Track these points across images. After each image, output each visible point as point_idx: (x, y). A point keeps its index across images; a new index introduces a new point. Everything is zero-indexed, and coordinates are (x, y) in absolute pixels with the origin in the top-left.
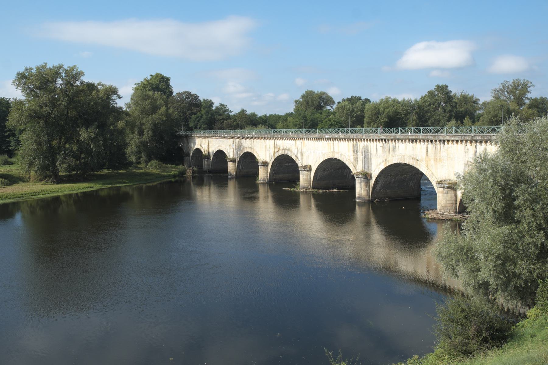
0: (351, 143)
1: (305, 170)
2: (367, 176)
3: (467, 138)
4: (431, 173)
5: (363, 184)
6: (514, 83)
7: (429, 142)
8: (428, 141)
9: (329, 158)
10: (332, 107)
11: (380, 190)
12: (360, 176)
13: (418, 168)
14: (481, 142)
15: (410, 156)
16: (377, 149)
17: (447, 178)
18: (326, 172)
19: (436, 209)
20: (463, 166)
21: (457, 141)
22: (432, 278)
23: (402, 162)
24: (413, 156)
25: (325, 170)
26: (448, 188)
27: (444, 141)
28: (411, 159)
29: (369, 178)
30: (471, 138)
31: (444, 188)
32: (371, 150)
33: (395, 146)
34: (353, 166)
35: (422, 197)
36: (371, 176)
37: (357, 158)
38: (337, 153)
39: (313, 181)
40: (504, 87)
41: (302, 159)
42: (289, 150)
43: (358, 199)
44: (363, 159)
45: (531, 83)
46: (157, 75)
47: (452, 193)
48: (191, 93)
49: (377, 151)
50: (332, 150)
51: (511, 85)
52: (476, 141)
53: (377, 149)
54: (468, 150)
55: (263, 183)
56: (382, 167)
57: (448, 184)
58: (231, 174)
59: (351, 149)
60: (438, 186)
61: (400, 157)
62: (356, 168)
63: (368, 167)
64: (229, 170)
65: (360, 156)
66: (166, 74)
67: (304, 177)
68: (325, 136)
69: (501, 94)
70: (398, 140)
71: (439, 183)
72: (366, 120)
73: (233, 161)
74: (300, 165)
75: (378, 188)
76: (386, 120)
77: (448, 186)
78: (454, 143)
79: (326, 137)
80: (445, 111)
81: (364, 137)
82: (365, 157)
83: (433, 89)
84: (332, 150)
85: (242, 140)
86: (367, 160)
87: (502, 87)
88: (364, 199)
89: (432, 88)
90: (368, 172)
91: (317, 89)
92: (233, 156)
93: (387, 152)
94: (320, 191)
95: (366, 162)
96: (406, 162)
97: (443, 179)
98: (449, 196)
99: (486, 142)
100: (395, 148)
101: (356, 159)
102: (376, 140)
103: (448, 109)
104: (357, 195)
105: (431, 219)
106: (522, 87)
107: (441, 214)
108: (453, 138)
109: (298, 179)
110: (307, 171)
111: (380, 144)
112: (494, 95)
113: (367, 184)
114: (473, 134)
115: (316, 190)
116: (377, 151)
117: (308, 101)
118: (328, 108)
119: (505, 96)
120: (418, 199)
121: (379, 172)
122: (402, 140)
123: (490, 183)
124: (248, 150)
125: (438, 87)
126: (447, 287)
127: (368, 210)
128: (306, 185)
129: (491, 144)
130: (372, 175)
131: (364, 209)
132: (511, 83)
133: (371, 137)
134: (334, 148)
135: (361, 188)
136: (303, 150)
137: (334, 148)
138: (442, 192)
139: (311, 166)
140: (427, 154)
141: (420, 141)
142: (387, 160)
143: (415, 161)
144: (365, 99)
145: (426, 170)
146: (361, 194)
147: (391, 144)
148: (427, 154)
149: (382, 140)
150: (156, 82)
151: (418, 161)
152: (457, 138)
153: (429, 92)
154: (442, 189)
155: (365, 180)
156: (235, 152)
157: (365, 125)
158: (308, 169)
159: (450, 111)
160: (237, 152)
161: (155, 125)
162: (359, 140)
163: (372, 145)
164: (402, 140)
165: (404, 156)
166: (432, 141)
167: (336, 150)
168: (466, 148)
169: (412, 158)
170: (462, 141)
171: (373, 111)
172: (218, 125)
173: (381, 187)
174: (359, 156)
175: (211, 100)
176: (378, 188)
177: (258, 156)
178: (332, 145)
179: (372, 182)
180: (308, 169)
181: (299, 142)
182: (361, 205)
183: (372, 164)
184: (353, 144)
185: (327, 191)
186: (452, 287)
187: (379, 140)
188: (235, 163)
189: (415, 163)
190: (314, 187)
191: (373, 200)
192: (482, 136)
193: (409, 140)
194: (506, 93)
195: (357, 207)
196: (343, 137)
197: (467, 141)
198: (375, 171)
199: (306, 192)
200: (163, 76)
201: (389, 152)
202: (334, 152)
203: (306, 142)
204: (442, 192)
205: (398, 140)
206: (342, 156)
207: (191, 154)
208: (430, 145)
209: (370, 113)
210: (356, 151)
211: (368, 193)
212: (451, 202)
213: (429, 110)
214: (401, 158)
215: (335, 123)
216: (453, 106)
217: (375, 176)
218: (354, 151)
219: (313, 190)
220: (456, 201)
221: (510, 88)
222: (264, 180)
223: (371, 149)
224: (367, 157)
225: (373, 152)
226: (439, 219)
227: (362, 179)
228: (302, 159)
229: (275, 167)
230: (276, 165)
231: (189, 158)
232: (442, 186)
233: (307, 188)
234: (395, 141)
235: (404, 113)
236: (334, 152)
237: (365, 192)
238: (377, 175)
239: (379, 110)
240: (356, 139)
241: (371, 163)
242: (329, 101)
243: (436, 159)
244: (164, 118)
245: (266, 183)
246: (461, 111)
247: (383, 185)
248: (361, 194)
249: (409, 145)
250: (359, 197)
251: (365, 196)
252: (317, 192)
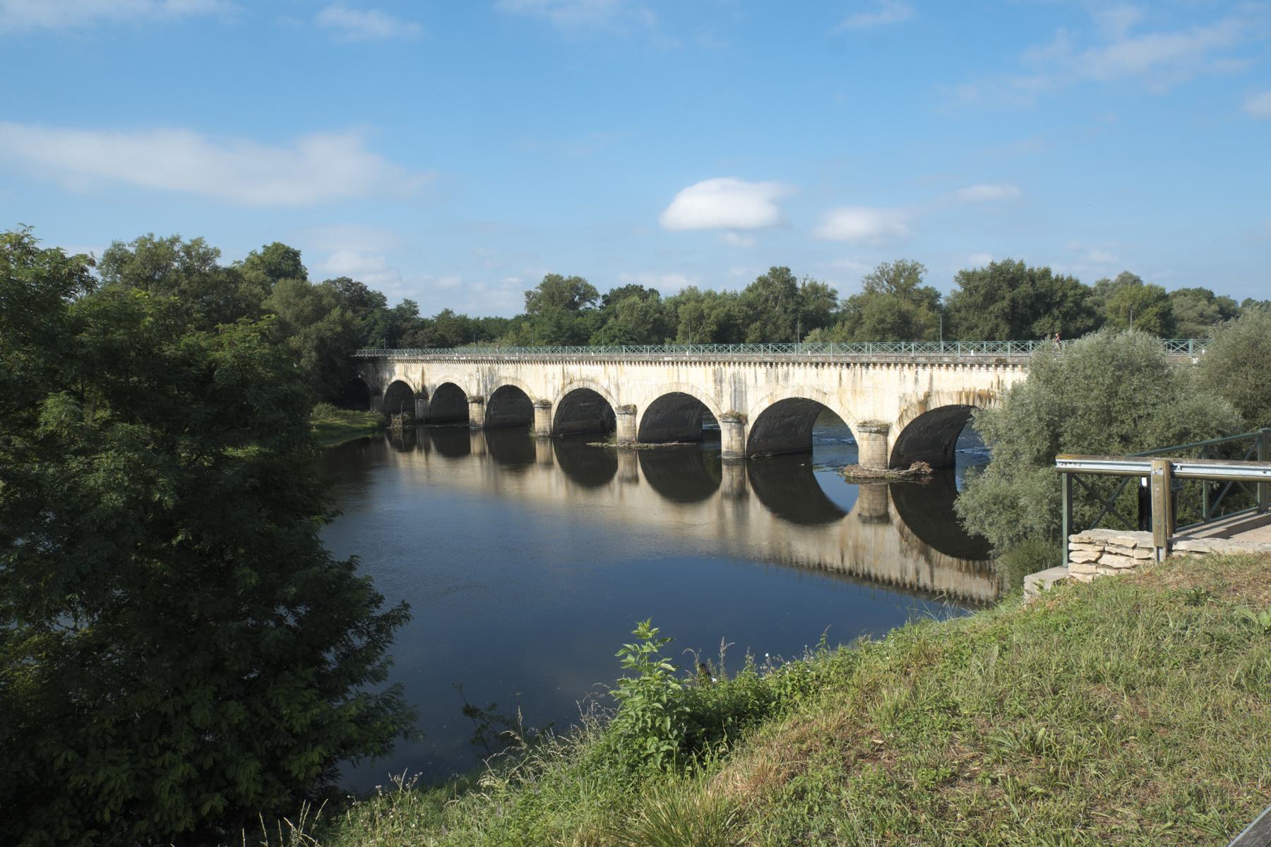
0: (710, 369)
1: (627, 413)
2: (740, 420)
3: (905, 360)
4: (846, 411)
5: (734, 431)
6: (897, 266)
7: (844, 366)
8: (842, 364)
9: (670, 392)
10: (594, 304)
11: (758, 440)
12: (730, 420)
13: (825, 404)
14: (925, 365)
17: (872, 419)
19: (858, 463)
20: (898, 400)
21: (889, 365)
22: (848, 564)
23: (800, 396)
25: (658, 412)
26: (877, 432)
27: (868, 365)
29: (744, 422)
30: (910, 360)
31: (871, 432)
32: (745, 380)
33: (788, 373)
34: (713, 404)
35: (814, 449)
36: (746, 418)
37: (721, 391)
38: (684, 384)
39: (640, 430)
40: (882, 272)
41: (618, 395)
42: (592, 380)
43: (727, 455)
45: (922, 266)
46: (277, 246)
49: (756, 381)
51: (892, 270)
52: (917, 365)
55: (544, 436)
56: (766, 404)
57: (877, 426)
58: (475, 424)
59: (711, 378)
60: (861, 430)
61: (796, 388)
62: (719, 407)
63: (741, 405)
64: (471, 417)
65: (727, 389)
66: (294, 246)
68: (663, 357)
69: (878, 284)
70: (794, 364)
71: (864, 425)
72: (680, 328)
73: (479, 400)
74: (614, 406)
75: (756, 436)
76: (714, 328)
78: (884, 367)
79: (666, 359)
80: (785, 312)
81: (735, 359)
82: (735, 390)
83: (766, 274)
84: (676, 380)
85: (496, 366)
86: (739, 394)
87: (879, 274)
88: (736, 454)
89: (764, 272)
90: (741, 412)
91: (567, 272)
92: (478, 393)
93: (774, 382)
94: (652, 445)
95: (737, 397)
96: (807, 396)
97: (867, 419)
99: (932, 365)
100: (786, 376)
101: (719, 394)
102: (755, 364)
103: (791, 307)
104: (724, 449)
105: (854, 478)
106: (909, 274)
107: (867, 470)
108: (883, 360)
109: (613, 427)
110: (630, 414)
111: (761, 370)
112: (865, 285)
113: (741, 432)
114: (913, 355)
115: (646, 445)
116: (756, 381)
117: (553, 294)
118: (588, 305)
119: (883, 286)
120: (809, 452)
121: (761, 411)
122: (799, 364)
123: (1034, 418)
124: (510, 383)
125: (774, 270)
126: (873, 575)
127: (743, 471)
128: (628, 436)
129: (987, 369)
130: (749, 418)
131: (736, 471)
132: (892, 266)
133: (747, 359)
134: (679, 376)
135: (732, 438)
136: (620, 382)
137: (679, 376)
138: (867, 439)
139: (635, 406)
140: (840, 384)
141: (829, 364)
144: (650, 290)
145: (839, 408)
146: (732, 447)
147: (781, 370)
148: (840, 384)
149: (766, 363)
150: (275, 258)
151: (826, 394)
152: (888, 360)
153: (760, 279)
154: (867, 434)
155: (738, 425)
156: (481, 386)
157: (679, 337)
158: (631, 410)
159: (794, 311)
161: (322, 340)
162: (724, 363)
163: (747, 372)
164: (799, 364)
165: (802, 387)
166: (848, 365)
167: (683, 379)
168: (902, 375)
170: (896, 365)
171: (693, 314)
172: (407, 338)
174: (724, 389)
175: (381, 293)
176: (756, 436)
177: (531, 391)
178: (675, 371)
179: (748, 428)
180: (630, 410)
181: (611, 369)
182: (731, 464)
183: (748, 401)
185: (664, 445)
186: (879, 575)
187: (760, 364)
188: (483, 404)
189: (820, 398)
190: (641, 439)
191: (749, 455)
192: (927, 358)
193: (811, 364)
194: (885, 283)
195: (724, 467)
196: (696, 359)
197: (903, 365)
198: (755, 408)
199: (630, 448)
200: (289, 248)
202: (678, 383)
203: (627, 368)
204: (867, 439)
205: (794, 364)
206: (694, 390)
207: (385, 391)
208: (845, 371)
209: (688, 317)
210: (719, 381)
211: (742, 445)
212: (880, 452)
213: (765, 309)
214: (798, 390)
215: (622, 333)
216: (798, 303)
217: (752, 417)
218: (715, 381)
219: (640, 444)
220: (887, 451)
221: (891, 274)
222: (545, 432)
223: (745, 377)
224: (738, 389)
225: (750, 381)
226: (866, 478)
227: (733, 424)
228: (618, 395)
232: (868, 429)
233: (630, 442)
234: (788, 364)
236: (678, 383)
237: (738, 443)
238: (756, 417)
239: (702, 311)
240: (719, 363)
241: (746, 400)
242: (589, 293)
243: (854, 392)
244: (339, 329)
245: (549, 437)
246: (812, 312)
248: (732, 447)
249: (812, 371)
250: (727, 452)
251: (738, 451)
252: (647, 447)
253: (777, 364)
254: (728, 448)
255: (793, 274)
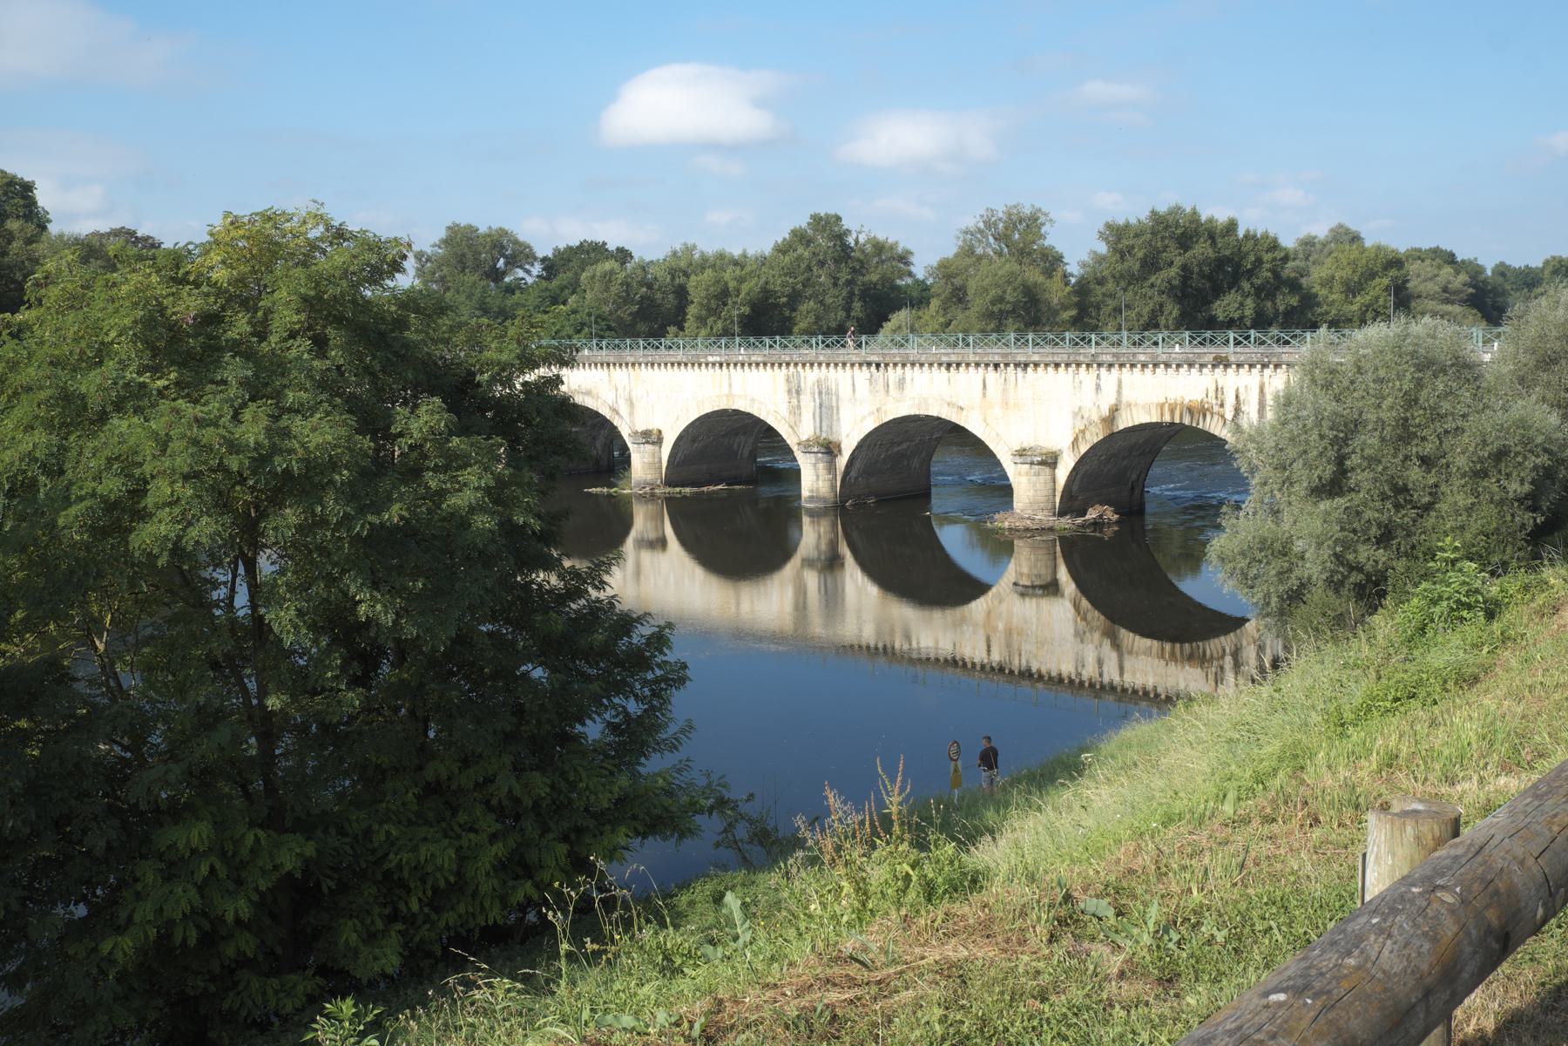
0: (780, 374)
1: (648, 442)
2: (830, 450)
3: (1081, 358)
5: (821, 466)
6: (1010, 215)
7: (991, 368)
8: (987, 365)
9: (716, 409)
10: (528, 272)
11: (856, 479)
12: (816, 450)
13: (962, 424)
14: (1111, 366)
15: (943, 400)
17: (1032, 444)
19: (1012, 508)
20: (1071, 416)
21: (1057, 365)
22: (996, 657)
23: (923, 412)
24: (949, 400)
25: (694, 440)
26: (1040, 463)
27: (1026, 365)
28: (946, 406)
29: (836, 452)
30: (1090, 358)
31: (1032, 463)
32: (837, 390)
33: (904, 378)
35: (933, 490)
36: (839, 447)
37: (799, 407)
39: (667, 468)
40: (988, 224)
41: (631, 414)
42: (588, 393)
43: (806, 502)
44: (815, 410)
45: (1046, 215)
48: (135, 232)
49: (854, 391)
50: (726, 391)
51: (1000, 219)
52: (1100, 365)
54: (1081, 382)
56: (870, 425)
57: (1041, 454)
59: (782, 387)
60: (1018, 460)
61: (917, 401)
62: (796, 429)
63: (831, 427)
65: (808, 405)
68: (706, 356)
69: (980, 241)
70: (913, 365)
71: (1021, 453)
72: (692, 310)
74: (625, 433)
75: (853, 474)
76: (746, 310)
78: (1050, 369)
79: (710, 359)
80: (835, 285)
81: (821, 358)
82: (821, 405)
83: (804, 225)
84: (726, 391)
86: (827, 408)
87: (981, 225)
88: (825, 500)
89: (802, 221)
90: (831, 438)
91: (485, 222)
93: (882, 392)
94: (687, 490)
95: (824, 416)
96: (933, 412)
97: (1026, 445)
99: (1122, 365)
100: (901, 383)
101: (796, 411)
102: (853, 365)
103: (844, 276)
105: (1010, 529)
106: (1028, 226)
107: (1029, 518)
108: (1048, 359)
109: (626, 461)
110: (653, 443)
111: (862, 375)
112: (961, 243)
113: (831, 467)
114: (1093, 351)
115: (678, 489)
116: (854, 391)
117: (463, 255)
118: (520, 273)
119: (989, 245)
120: (925, 495)
121: (862, 436)
122: (922, 365)
125: (816, 219)
126: (1034, 670)
127: (834, 525)
128: (649, 477)
130: (843, 446)
131: (824, 526)
132: (1001, 215)
133: (841, 359)
134: (730, 385)
135: (818, 477)
136: (634, 395)
137: (730, 385)
138: (1027, 474)
139: (660, 432)
140: (984, 395)
141: (968, 365)
142: (884, 409)
144: (618, 249)
146: (818, 489)
147: (893, 374)
148: (984, 395)
149: (869, 364)
151: (962, 409)
152: (1057, 359)
153: (794, 233)
154: (1027, 466)
155: (826, 458)
157: (690, 324)
158: (654, 438)
159: (849, 283)
162: (804, 365)
163: (839, 378)
164: (922, 365)
166: (996, 366)
168: (1077, 380)
169: (948, 404)
170: (1068, 365)
171: (712, 289)
174: (803, 404)
176: (853, 474)
179: (842, 461)
180: (651, 438)
181: (619, 374)
182: (815, 514)
183: (841, 420)
184: (788, 376)
185: (705, 489)
186: (1044, 671)
187: (861, 365)
189: (954, 415)
190: (670, 482)
191: (843, 502)
192: (1114, 355)
193: (940, 365)
194: (991, 240)
195: (806, 520)
196: (760, 359)
197: (1078, 365)
198: (850, 436)
199: (653, 495)
200: (14, 177)
201: (887, 391)
202: (729, 396)
203: (645, 373)
204: (1027, 474)
205: (913, 365)
208: (991, 374)
209: (703, 294)
210: (795, 391)
211: (833, 487)
212: (1046, 493)
213: (809, 280)
215: (593, 318)
216: (854, 270)
217: (848, 447)
218: (789, 391)
219: (668, 490)
220: (1054, 490)
221: (1001, 226)
223: (837, 385)
224: (826, 403)
225: (845, 392)
226: (1027, 530)
227: (820, 455)
228: (631, 414)
232: (1029, 460)
233: (653, 486)
234: (904, 365)
235: (786, 293)
236: (729, 396)
237: (827, 484)
238: (855, 444)
239: (726, 283)
240: (796, 364)
241: (838, 419)
242: (520, 255)
243: (1005, 404)
246: (875, 284)
248: (818, 489)
249: (940, 375)
250: (811, 497)
251: (826, 495)
252: (680, 493)
253: (887, 365)
254: (812, 491)
255: (846, 223)
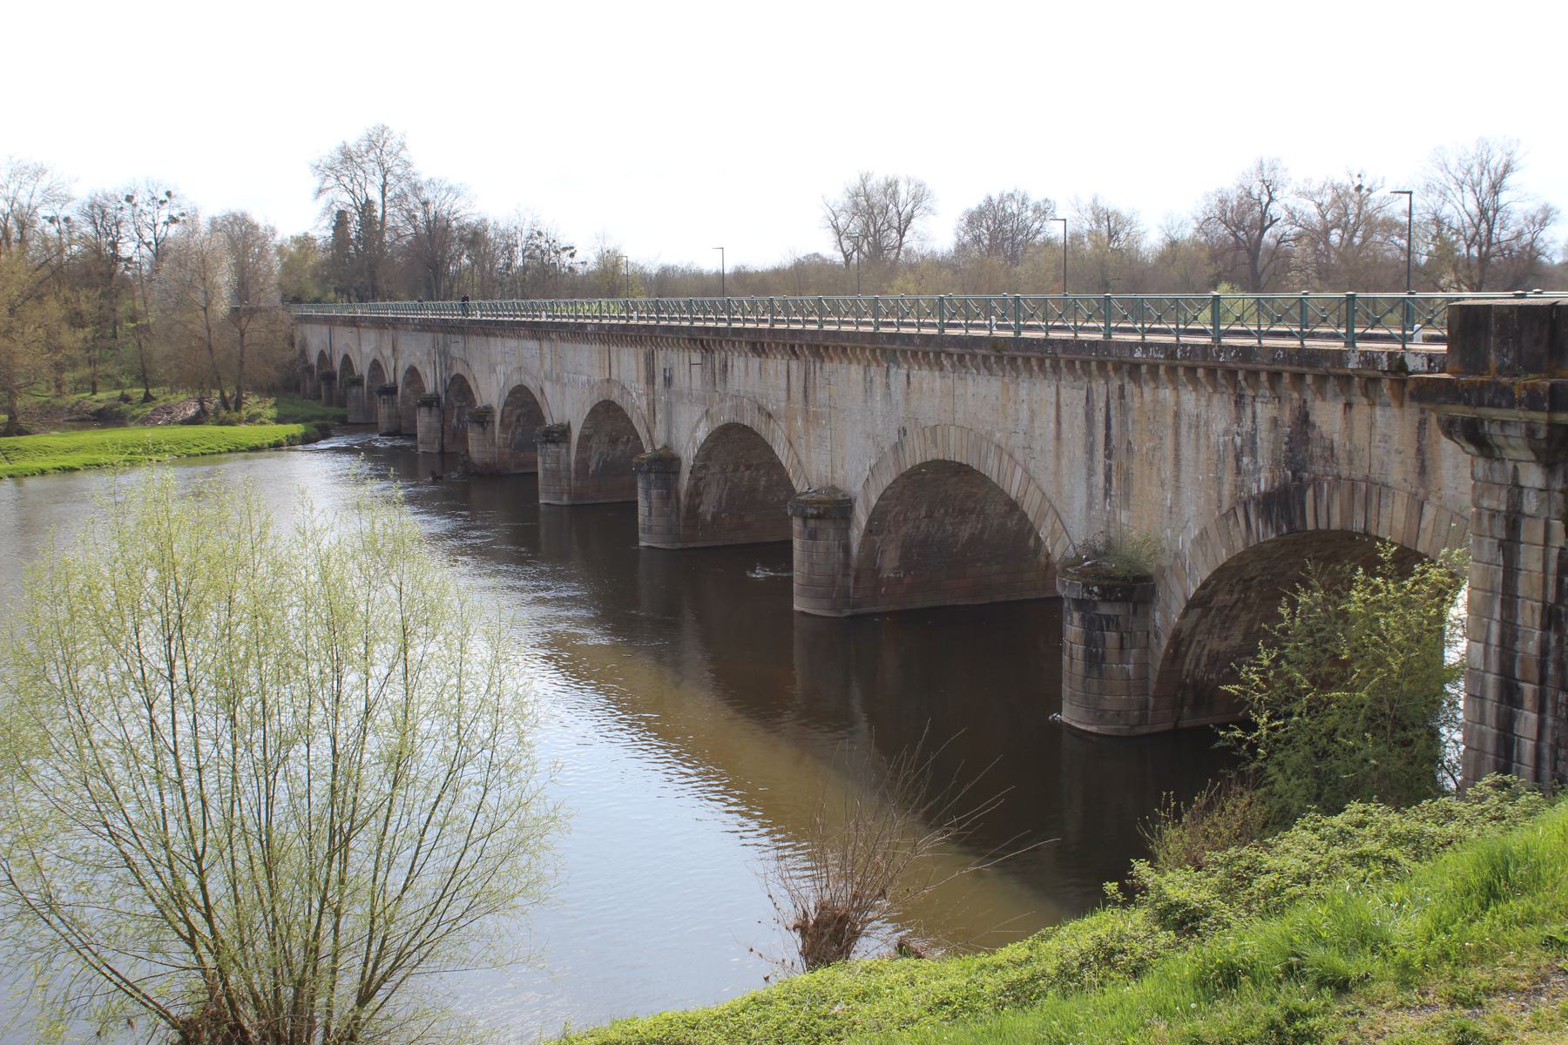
16: (788, 377)
18: (620, 448)
47: (832, 537)
50: (607, 376)
53: (788, 377)
54: (871, 381)
67: (547, 465)
77: (815, 512)
84: (607, 376)
92: (436, 388)
98: (821, 550)
143: (764, 419)
151: (769, 416)
160: (441, 375)
173: (720, 502)
177: (477, 387)
229: (516, 427)
230: (518, 420)
231: (360, 390)
247: (724, 497)
